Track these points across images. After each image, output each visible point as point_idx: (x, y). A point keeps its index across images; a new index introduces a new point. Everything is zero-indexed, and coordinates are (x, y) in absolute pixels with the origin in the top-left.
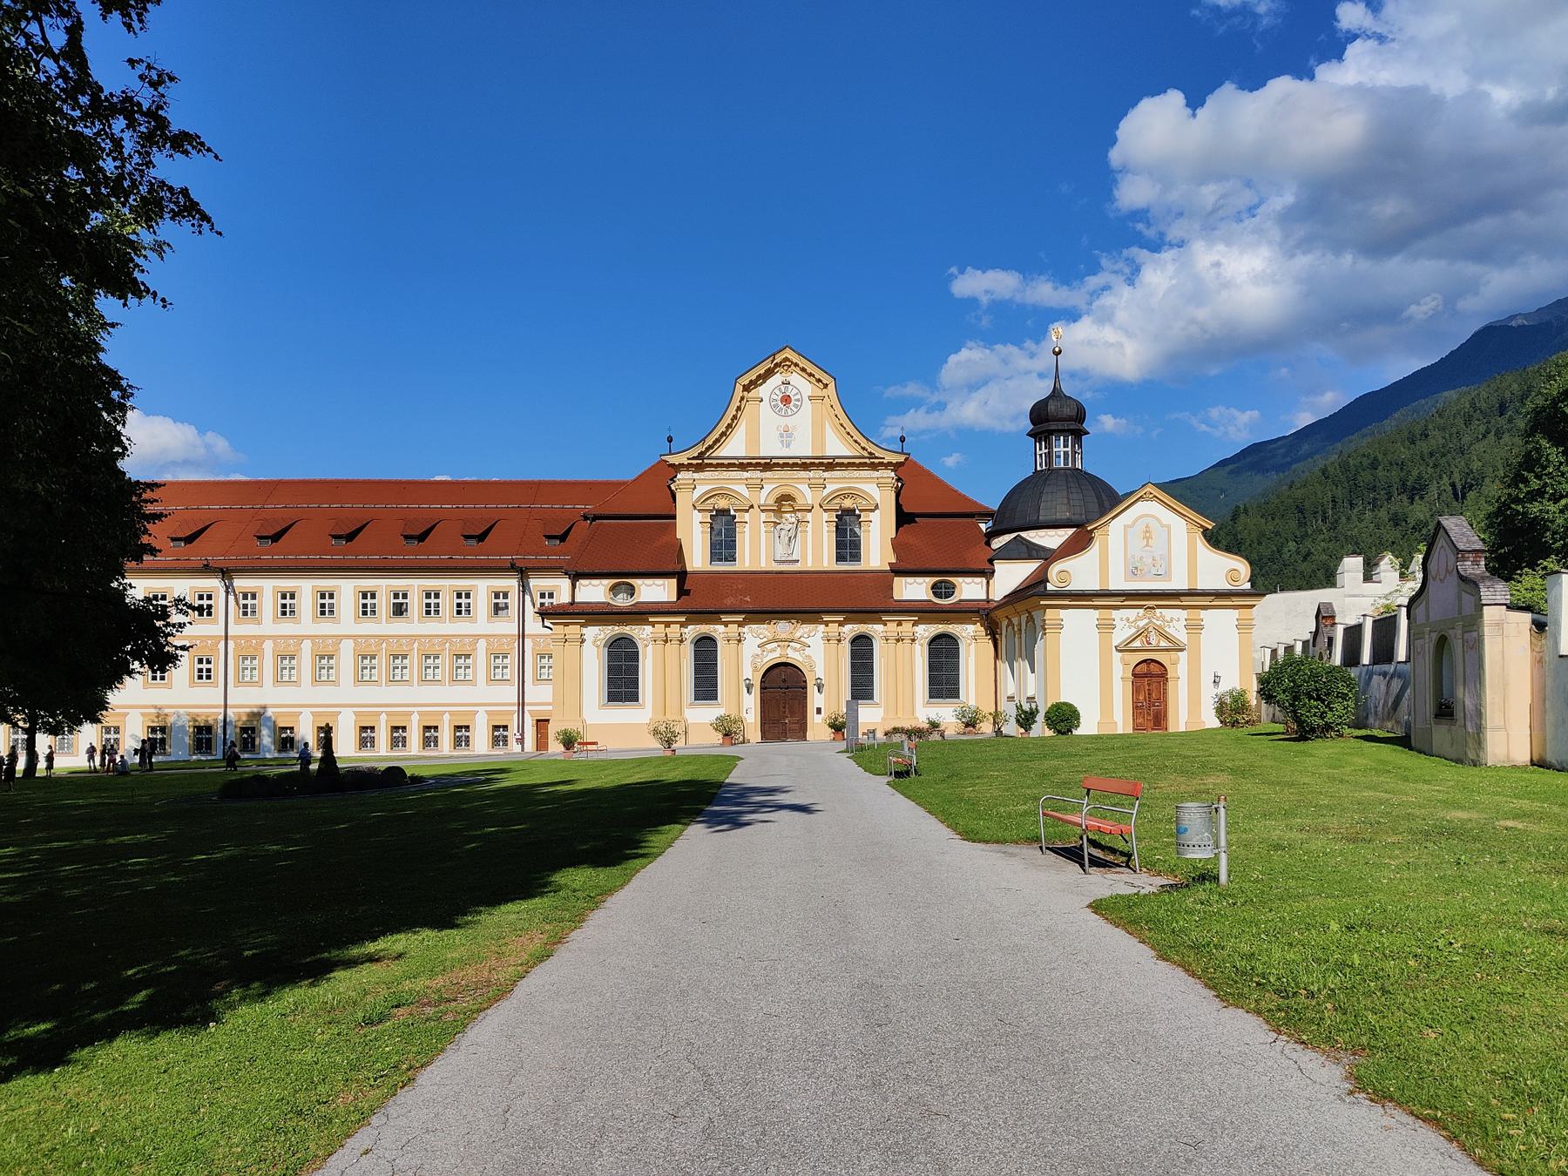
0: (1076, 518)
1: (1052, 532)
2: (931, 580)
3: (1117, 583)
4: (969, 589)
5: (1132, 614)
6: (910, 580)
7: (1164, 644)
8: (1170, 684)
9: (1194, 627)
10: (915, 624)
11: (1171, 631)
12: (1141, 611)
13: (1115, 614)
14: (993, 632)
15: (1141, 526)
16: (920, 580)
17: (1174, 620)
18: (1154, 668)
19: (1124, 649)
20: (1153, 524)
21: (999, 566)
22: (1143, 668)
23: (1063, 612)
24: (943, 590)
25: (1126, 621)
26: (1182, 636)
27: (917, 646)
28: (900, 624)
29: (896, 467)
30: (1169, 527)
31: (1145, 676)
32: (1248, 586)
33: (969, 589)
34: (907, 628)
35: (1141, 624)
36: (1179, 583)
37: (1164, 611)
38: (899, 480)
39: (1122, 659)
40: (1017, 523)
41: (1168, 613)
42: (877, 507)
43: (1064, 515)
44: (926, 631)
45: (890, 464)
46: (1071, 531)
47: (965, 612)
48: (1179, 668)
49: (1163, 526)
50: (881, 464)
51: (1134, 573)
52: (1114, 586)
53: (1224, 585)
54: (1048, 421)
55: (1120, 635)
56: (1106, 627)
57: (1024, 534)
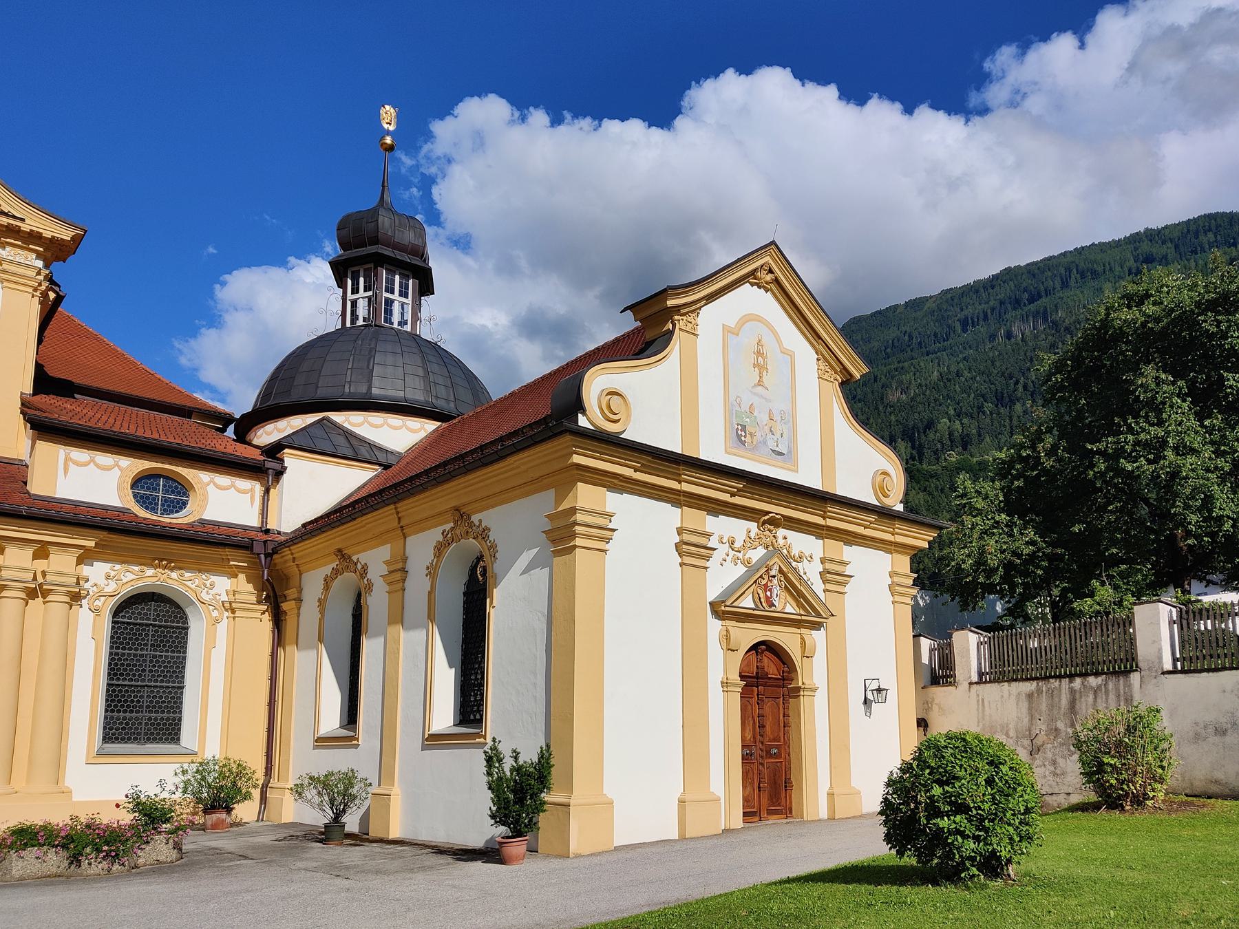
0: (442, 405)
1: (396, 420)
2: (132, 465)
4: (223, 500)
6: (80, 454)
7: (791, 608)
9: (835, 576)
10: (86, 557)
14: (276, 596)
15: (747, 339)
21: (293, 461)
24: (157, 490)
27: (84, 614)
28: (42, 552)
29: (55, 252)
32: (900, 508)
33: (223, 500)
34: (61, 564)
35: (756, 554)
36: (809, 478)
40: (325, 392)
41: (799, 542)
43: (416, 393)
44: (111, 579)
46: (431, 426)
47: (213, 544)
49: (784, 352)
51: (740, 436)
54: (375, 241)
55: (721, 576)
56: (692, 550)
57: (338, 417)
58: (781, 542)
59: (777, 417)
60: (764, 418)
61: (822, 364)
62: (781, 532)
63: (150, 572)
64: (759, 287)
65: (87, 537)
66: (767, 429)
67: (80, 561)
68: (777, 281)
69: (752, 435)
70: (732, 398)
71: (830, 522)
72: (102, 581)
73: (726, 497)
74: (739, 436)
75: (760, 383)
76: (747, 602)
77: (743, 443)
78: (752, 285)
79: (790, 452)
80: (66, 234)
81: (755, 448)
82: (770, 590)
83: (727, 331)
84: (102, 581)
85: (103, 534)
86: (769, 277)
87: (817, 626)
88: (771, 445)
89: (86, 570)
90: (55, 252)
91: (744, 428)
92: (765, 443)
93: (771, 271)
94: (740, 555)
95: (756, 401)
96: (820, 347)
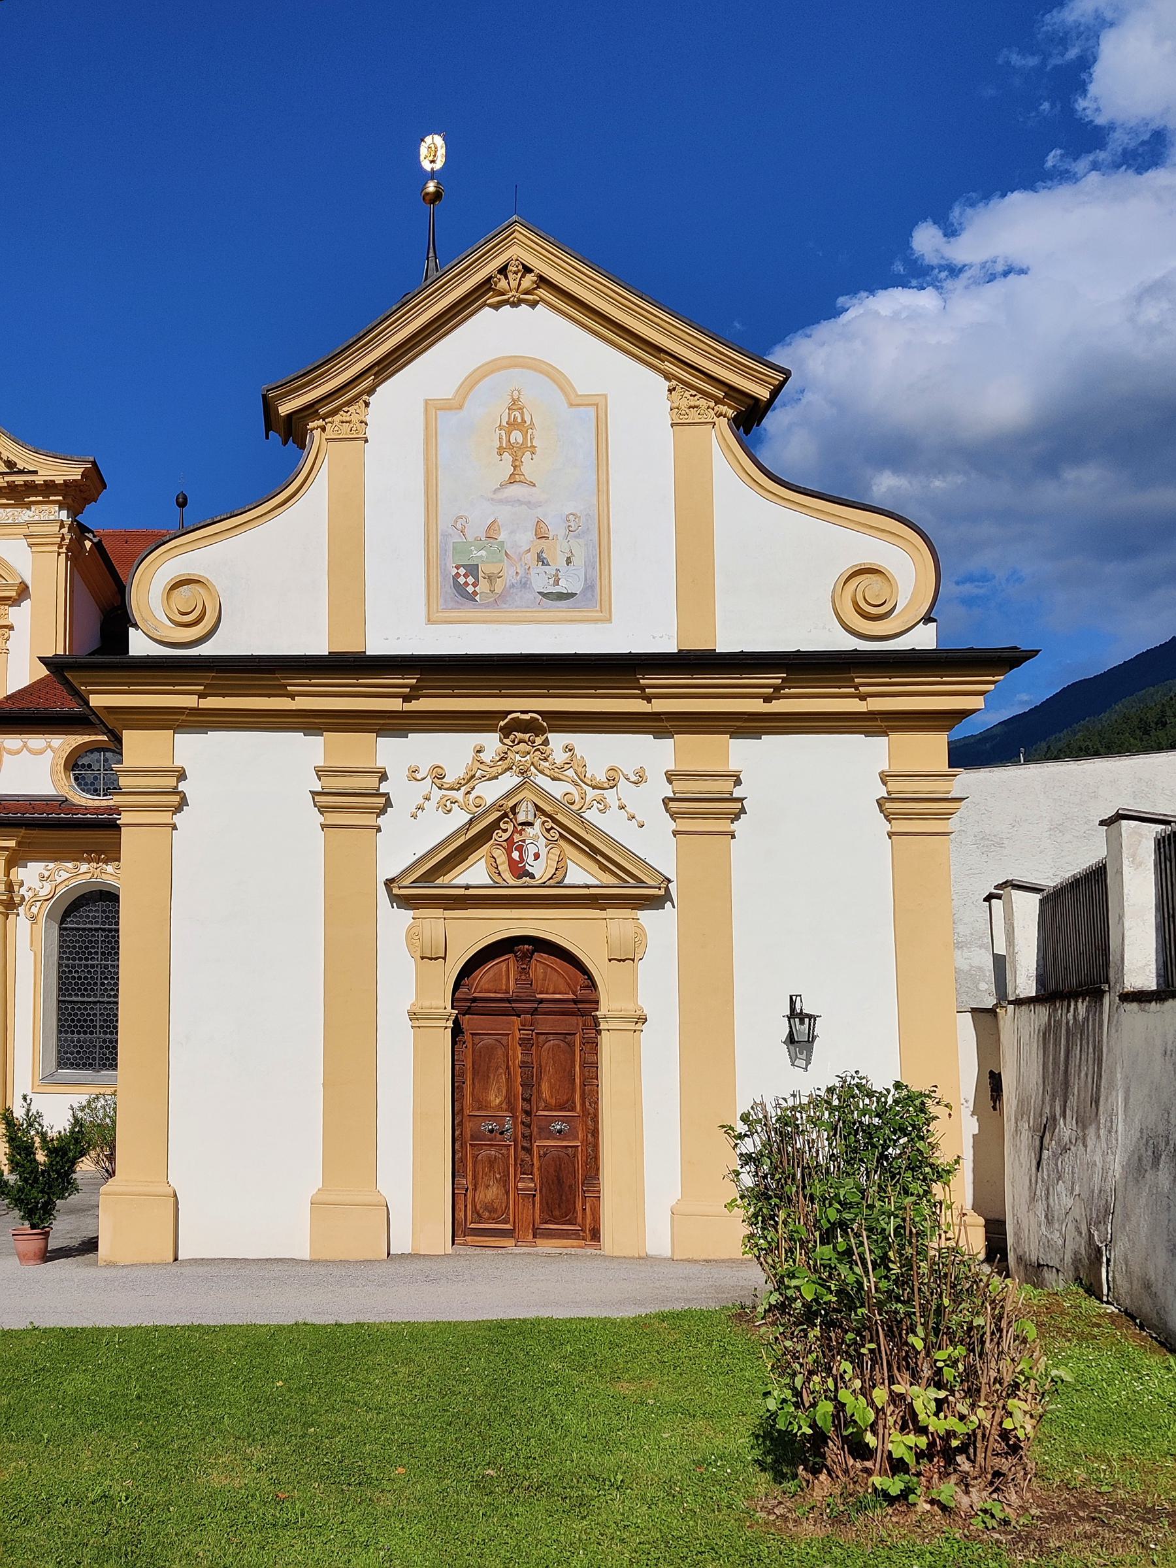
2: (62, 744)
3: (401, 625)
5: (454, 751)
7: (581, 874)
8: (611, 1046)
11: (609, 823)
12: (491, 742)
13: (394, 754)
15: (488, 407)
16: (37, 741)
17: (624, 780)
18: (546, 976)
19: (425, 889)
20: (541, 402)
22: (501, 976)
23: (189, 748)
25: (432, 779)
26: (648, 836)
30: (598, 406)
31: (507, 1007)
35: (491, 792)
36: (642, 625)
37: (587, 744)
38: (80, 530)
39: (412, 937)
41: (598, 751)
42: (23, 592)
45: (49, 488)
48: (644, 976)
50: (31, 488)
51: (463, 586)
52: (376, 646)
53: (834, 639)
58: (560, 757)
59: (555, 528)
60: (526, 538)
61: (685, 398)
62: (558, 740)
63: (84, 867)
64: (515, 305)
65: (9, 837)
66: (531, 558)
67: (10, 864)
68: (543, 281)
69: (490, 578)
70: (444, 522)
71: (659, 706)
72: (37, 884)
73: (395, 705)
74: (460, 589)
75: (512, 480)
76: (474, 874)
77: (472, 597)
78: (497, 306)
79: (589, 587)
80: (73, 472)
81: (498, 600)
82: (520, 849)
83: (433, 408)
84: (37, 884)
85: (22, 831)
86: (528, 281)
87: (655, 902)
88: (541, 581)
89: (19, 874)
90: (76, 496)
91: (472, 570)
92: (525, 585)
93: (527, 270)
94: (459, 795)
95: (503, 514)
96: (668, 366)
